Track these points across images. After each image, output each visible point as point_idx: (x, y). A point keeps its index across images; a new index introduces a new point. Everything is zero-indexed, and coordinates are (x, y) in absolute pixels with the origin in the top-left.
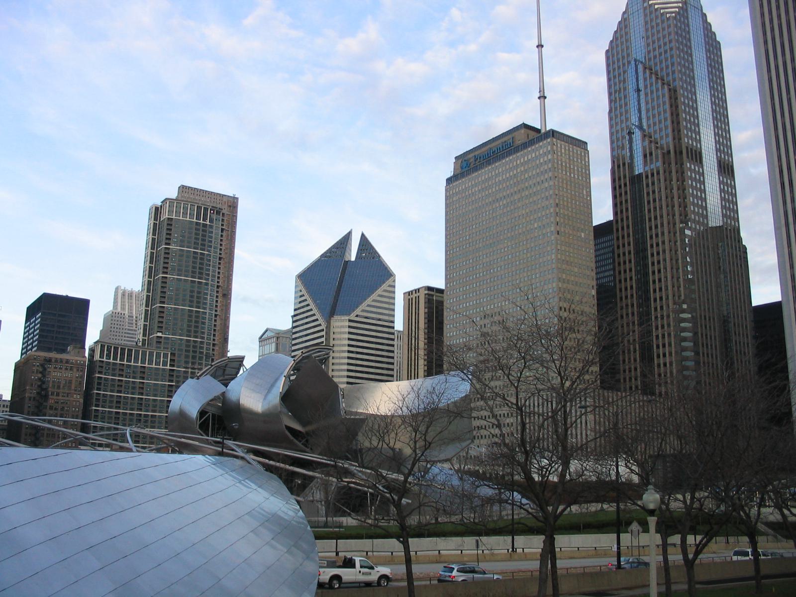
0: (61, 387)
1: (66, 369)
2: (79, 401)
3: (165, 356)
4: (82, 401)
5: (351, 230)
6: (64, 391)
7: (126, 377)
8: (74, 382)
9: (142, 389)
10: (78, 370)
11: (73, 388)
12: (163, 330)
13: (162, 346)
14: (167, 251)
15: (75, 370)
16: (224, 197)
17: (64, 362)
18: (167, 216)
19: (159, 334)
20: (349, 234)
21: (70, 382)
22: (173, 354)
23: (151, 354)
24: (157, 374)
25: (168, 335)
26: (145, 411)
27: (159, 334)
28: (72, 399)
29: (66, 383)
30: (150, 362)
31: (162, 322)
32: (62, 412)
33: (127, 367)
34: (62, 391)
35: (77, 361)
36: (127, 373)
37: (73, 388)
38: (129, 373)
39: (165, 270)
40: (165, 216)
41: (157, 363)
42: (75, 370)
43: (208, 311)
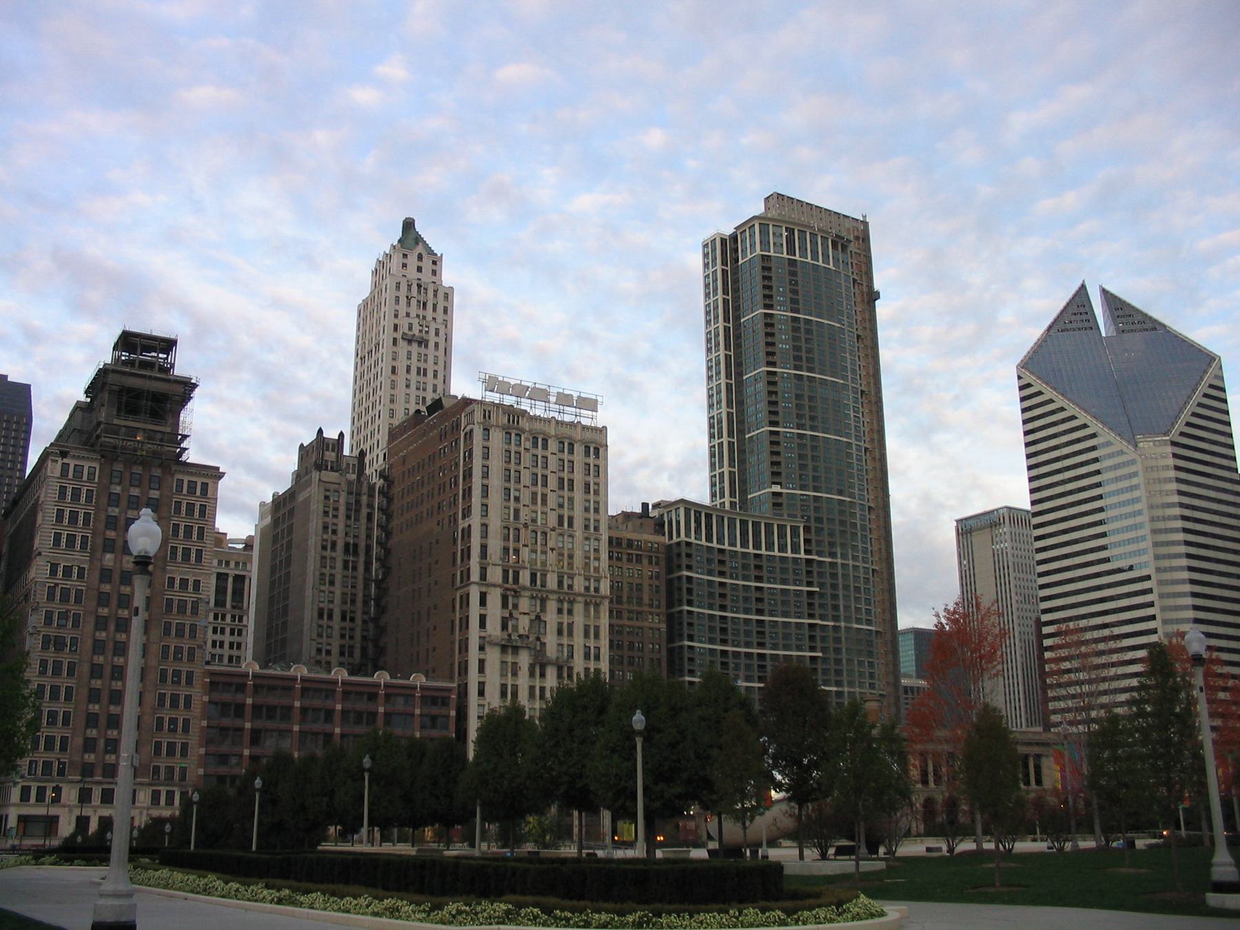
0: (625, 599)
1: (630, 560)
2: (659, 629)
3: (795, 530)
4: (663, 627)
5: (1084, 281)
6: (632, 608)
7: (732, 578)
8: (646, 588)
9: (759, 601)
10: (650, 563)
11: (646, 600)
12: (783, 479)
13: (785, 512)
14: (769, 321)
15: (645, 561)
16: (846, 220)
17: (624, 544)
18: (758, 251)
19: (776, 488)
20: (1083, 287)
21: (639, 588)
22: (807, 530)
23: (782, 528)
24: (783, 569)
25: (793, 489)
26: (772, 649)
27: (776, 488)
28: (645, 624)
29: (631, 589)
30: (770, 547)
31: (778, 464)
32: (631, 654)
33: (731, 557)
34: (625, 606)
35: (646, 542)
36: (731, 568)
37: (646, 600)
38: (736, 568)
39: (770, 359)
40: (750, 254)
41: (782, 548)
42: (645, 561)
43: (853, 441)
